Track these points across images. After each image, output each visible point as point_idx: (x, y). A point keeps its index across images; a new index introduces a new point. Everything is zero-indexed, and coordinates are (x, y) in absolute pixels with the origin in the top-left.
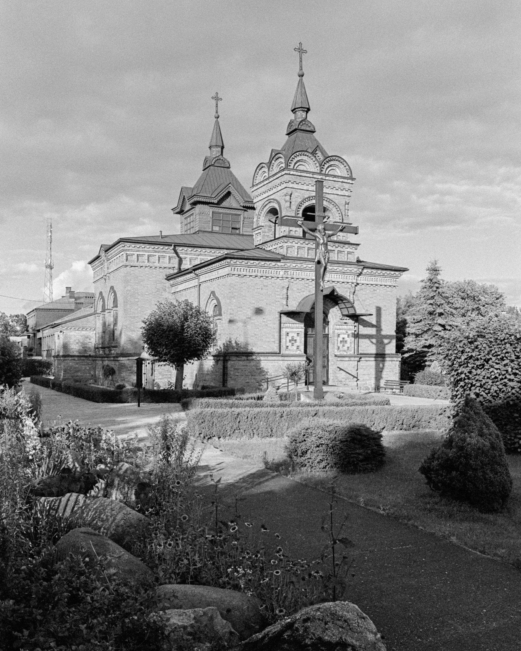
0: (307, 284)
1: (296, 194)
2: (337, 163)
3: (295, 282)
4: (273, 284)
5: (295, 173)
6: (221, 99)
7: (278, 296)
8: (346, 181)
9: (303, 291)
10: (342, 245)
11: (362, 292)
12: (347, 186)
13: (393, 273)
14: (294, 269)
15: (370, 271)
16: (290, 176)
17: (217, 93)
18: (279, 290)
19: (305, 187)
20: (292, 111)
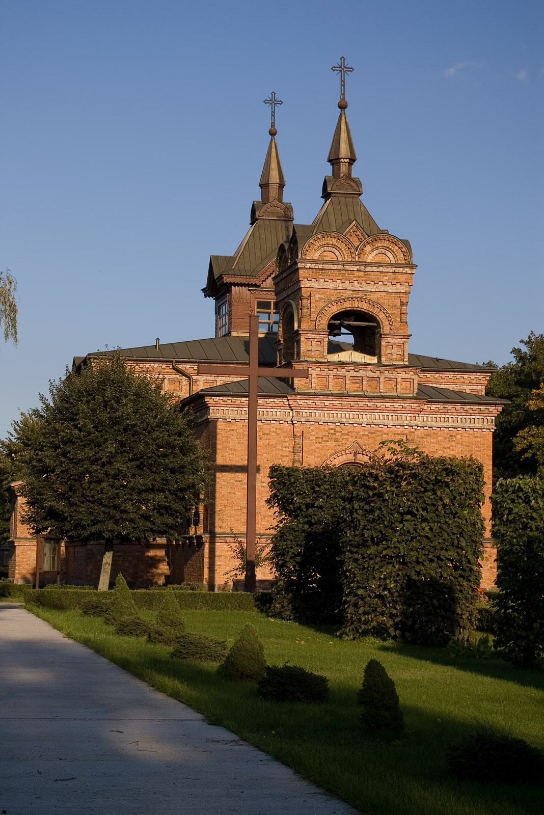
0: (332, 429)
1: (317, 296)
2: (386, 244)
3: (312, 428)
4: (279, 432)
5: (313, 266)
6: (281, 103)
7: (286, 449)
8: (398, 270)
9: (327, 441)
10: (391, 369)
11: (429, 439)
12: (402, 278)
13: (482, 408)
14: (309, 407)
15: (440, 406)
16: (307, 271)
17: (274, 93)
18: (287, 440)
19: (331, 285)
20: (330, 161)
